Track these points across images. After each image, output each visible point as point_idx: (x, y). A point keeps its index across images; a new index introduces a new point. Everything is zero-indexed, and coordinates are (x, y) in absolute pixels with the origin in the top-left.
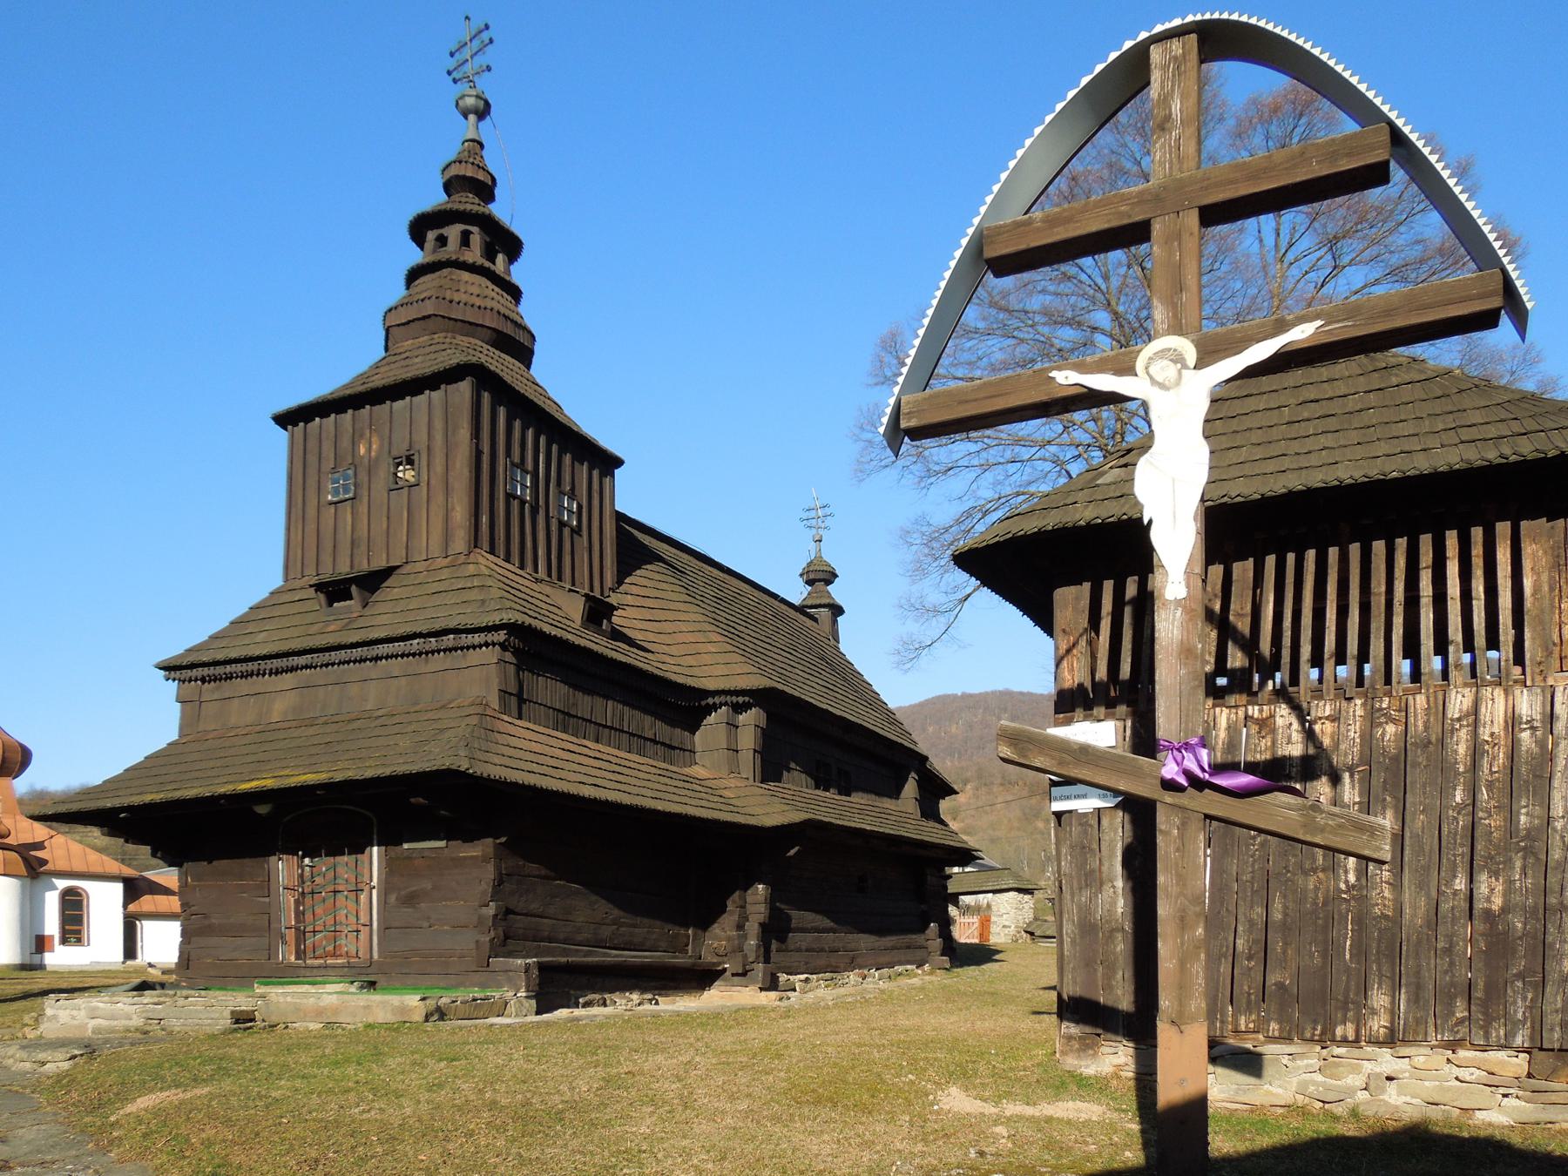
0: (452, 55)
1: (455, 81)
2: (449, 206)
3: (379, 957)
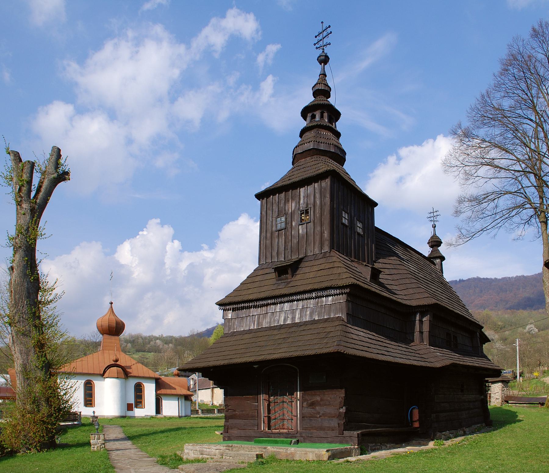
0: (316, 37)
1: (317, 48)
2: (316, 103)
3: (300, 430)
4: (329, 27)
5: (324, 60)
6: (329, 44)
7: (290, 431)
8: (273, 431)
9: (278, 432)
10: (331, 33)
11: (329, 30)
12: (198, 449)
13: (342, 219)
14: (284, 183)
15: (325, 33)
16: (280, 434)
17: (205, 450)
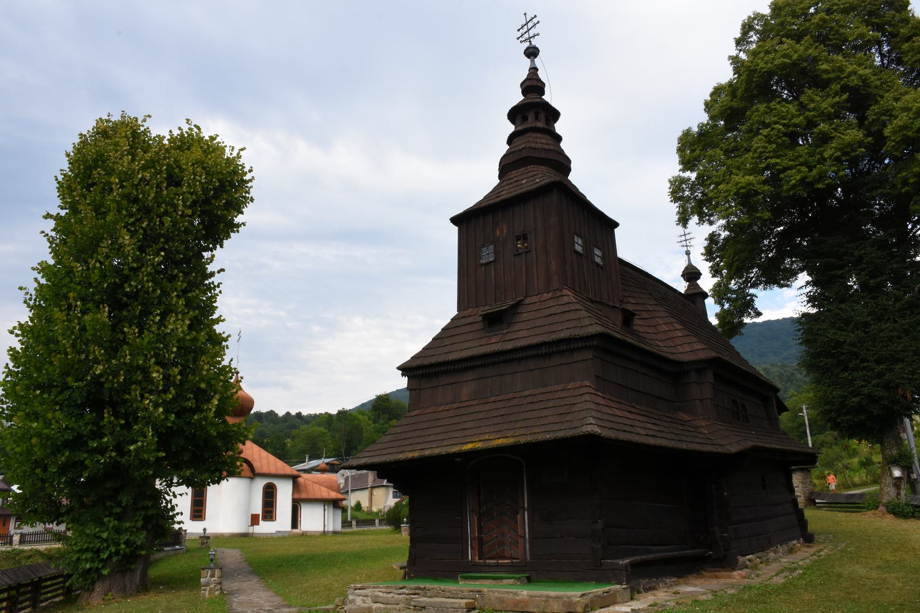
0: (519, 30)
1: (521, 42)
2: (527, 101)
3: (531, 558)
4: (535, 16)
5: (532, 53)
6: (538, 35)
7: (514, 561)
8: (487, 561)
9: (495, 563)
10: (538, 22)
11: (535, 20)
12: (370, 594)
13: (574, 245)
14: (491, 202)
15: (530, 25)
16: (498, 565)
17: (381, 594)
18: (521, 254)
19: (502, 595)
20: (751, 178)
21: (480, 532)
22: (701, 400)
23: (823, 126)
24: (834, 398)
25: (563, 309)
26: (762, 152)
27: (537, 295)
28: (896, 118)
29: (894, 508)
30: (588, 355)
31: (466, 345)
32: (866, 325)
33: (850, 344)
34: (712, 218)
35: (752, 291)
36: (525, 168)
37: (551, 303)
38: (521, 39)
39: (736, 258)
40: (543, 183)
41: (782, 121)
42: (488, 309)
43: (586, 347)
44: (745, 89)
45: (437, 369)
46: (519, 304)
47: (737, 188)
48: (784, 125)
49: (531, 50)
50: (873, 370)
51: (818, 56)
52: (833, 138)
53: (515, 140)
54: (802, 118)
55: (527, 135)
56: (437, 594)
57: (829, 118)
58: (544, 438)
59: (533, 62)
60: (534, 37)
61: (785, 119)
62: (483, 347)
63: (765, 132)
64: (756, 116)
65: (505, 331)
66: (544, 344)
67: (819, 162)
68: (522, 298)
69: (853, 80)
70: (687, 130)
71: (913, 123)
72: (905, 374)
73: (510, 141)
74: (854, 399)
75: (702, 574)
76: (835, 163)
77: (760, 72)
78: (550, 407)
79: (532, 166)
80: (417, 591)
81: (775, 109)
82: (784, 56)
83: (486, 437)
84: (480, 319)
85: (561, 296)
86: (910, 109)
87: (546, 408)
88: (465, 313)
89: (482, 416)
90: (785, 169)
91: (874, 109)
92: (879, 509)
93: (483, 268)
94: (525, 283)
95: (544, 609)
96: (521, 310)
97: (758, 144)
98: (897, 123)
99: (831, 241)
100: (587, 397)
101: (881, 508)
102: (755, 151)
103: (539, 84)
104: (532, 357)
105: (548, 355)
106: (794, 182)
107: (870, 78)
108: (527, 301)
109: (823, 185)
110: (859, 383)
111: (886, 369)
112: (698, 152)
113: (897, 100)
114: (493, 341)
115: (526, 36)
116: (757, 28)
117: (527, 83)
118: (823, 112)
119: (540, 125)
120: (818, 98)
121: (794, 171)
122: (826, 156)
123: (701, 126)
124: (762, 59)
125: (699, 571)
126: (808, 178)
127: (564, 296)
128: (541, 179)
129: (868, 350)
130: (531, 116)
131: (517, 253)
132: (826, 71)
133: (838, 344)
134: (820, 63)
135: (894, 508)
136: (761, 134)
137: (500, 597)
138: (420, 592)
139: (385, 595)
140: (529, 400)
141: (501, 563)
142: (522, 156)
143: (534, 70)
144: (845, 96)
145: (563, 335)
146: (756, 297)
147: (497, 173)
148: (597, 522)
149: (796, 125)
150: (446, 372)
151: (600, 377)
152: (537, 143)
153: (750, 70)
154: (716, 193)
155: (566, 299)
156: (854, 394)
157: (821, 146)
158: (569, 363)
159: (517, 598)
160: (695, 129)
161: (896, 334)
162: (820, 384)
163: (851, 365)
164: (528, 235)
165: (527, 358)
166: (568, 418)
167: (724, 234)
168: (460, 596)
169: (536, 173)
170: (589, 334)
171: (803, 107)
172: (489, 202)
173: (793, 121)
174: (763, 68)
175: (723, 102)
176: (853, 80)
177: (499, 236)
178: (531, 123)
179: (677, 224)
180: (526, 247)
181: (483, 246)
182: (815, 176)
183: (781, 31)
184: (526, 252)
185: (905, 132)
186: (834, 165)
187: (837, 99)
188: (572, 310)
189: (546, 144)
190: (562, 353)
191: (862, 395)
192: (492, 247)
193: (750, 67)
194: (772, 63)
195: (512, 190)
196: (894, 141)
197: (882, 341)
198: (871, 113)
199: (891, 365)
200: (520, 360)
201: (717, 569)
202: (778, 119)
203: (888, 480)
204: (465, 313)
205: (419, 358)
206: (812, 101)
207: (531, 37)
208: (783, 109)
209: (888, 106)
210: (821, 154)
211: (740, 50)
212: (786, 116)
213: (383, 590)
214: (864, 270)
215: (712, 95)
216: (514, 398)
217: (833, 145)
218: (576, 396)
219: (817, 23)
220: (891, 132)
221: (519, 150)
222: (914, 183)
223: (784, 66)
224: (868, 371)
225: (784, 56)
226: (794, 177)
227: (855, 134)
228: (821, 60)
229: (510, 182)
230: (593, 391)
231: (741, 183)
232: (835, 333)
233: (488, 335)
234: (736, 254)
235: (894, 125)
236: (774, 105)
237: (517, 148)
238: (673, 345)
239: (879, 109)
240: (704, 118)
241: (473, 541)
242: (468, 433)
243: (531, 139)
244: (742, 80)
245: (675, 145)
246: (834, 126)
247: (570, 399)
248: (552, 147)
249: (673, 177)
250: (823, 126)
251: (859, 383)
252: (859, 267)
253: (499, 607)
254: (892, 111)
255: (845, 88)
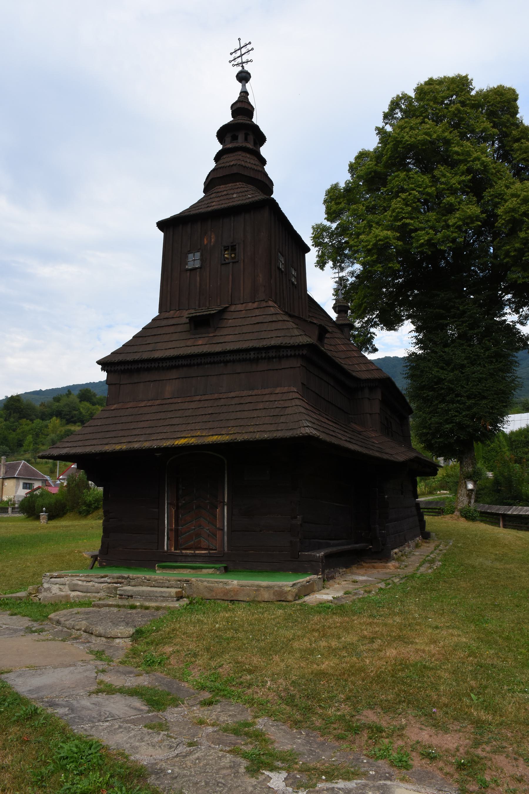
0: (231, 54)
1: (234, 65)
2: (236, 122)
3: (228, 550)
4: (250, 43)
6: (251, 61)
7: (211, 552)
8: (184, 551)
9: (192, 553)
10: (252, 49)
11: (249, 47)
12: (68, 582)
15: (244, 50)
16: (195, 556)
17: (80, 583)
18: (229, 263)
19: (212, 585)
20: (389, 233)
21: (177, 524)
22: (370, 414)
23: (452, 199)
24: (431, 423)
25: (270, 319)
26: (399, 212)
27: (242, 304)
28: (506, 201)
29: (467, 513)
30: (297, 363)
31: (170, 345)
32: (463, 366)
33: (450, 381)
34: (343, 265)
35: (372, 330)
36: (233, 184)
37: (257, 312)
38: (233, 62)
39: (365, 300)
40: (253, 199)
41: (418, 189)
42: (193, 312)
43: (295, 356)
44: (390, 157)
45: (140, 366)
46: (224, 311)
47: (376, 240)
48: (419, 192)
49: (244, 74)
50: (464, 403)
51: (451, 139)
52: (458, 210)
53: (224, 157)
54: (434, 188)
55: (236, 153)
56: (142, 583)
57: (453, 191)
58: (262, 437)
59: (244, 86)
60: (247, 62)
61: (420, 188)
62: (189, 348)
63: (403, 195)
64: (396, 181)
65: (212, 335)
66: (254, 349)
67: (443, 228)
68: (227, 305)
69: (477, 164)
70: (335, 184)
71: (519, 208)
72: (488, 408)
73: (218, 158)
74: (447, 426)
75: (362, 565)
76: (456, 230)
77: (405, 143)
78: (260, 409)
79: (240, 183)
80: (120, 580)
81: (413, 178)
82: (426, 134)
83: (198, 433)
84: (187, 321)
85: (267, 307)
86: (519, 196)
87: (257, 410)
88: (167, 315)
89: (188, 413)
90: (416, 230)
91: (490, 192)
92: (455, 513)
93: (188, 274)
94: (230, 291)
95: (254, 597)
96: (227, 316)
97: (396, 204)
98: (508, 205)
99: (443, 295)
100: (298, 402)
101: (457, 513)
102: (393, 211)
103: (250, 108)
104: (240, 361)
105: (256, 360)
106: (422, 241)
107: (490, 165)
108: (233, 308)
109: (445, 247)
110: (452, 412)
111: (474, 404)
112: (343, 205)
113: (507, 187)
114: (200, 342)
115: (239, 60)
116: (403, 107)
117: (239, 105)
118: (451, 187)
119: (250, 146)
120: (448, 174)
121: (423, 232)
122: (451, 224)
123: (347, 183)
124: (408, 133)
125: (359, 562)
126: (433, 240)
127: (270, 307)
128: (253, 195)
129: (463, 387)
130: (241, 137)
131: (224, 262)
132: (457, 153)
133: (440, 381)
134: (453, 145)
135: (467, 513)
136: (399, 197)
137: (209, 586)
138: (123, 581)
139: (85, 583)
140: (236, 401)
141: (198, 553)
142: (232, 172)
143: (244, 94)
144: (469, 177)
145: (273, 342)
146: (376, 335)
147: (202, 187)
148: (296, 518)
149: (428, 194)
150: (149, 370)
151: (304, 385)
152: (246, 162)
153: (396, 141)
154: (356, 242)
155: (272, 311)
156: (447, 422)
157: (446, 216)
158: (277, 370)
159: (227, 587)
160: (342, 185)
161: (484, 376)
162: (420, 411)
163: (448, 398)
164: (237, 246)
165: (234, 361)
166: (283, 419)
167: (351, 280)
168: (166, 585)
169: (246, 189)
170: (301, 344)
171: (435, 180)
172: (200, 211)
173: (426, 190)
174: (408, 141)
175: (369, 165)
176: (477, 164)
177: (207, 244)
178: (240, 142)
179: (316, 266)
180: (233, 258)
181: (190, 252)
182: (439, 239)
183: (424, 113)
184: (233, 263)
185: (513, 214)
186: (456, 232)
187: (463, 178)
188: (279, 321)
189: (255, 164)
190: (270, 359)
191: (454, 423)
192: (198, 255)
193: (397, 138)
194: (416, 139)
195: (223, 202)
196: (504, 219)
197: (474, 381)
198: (487, 194)
199: (478, 400)
200: (226, 363)
201: (374, 561)
202: (415, 186)
203: (463, 492)
204: (167, 315)
205: (121, 353)
206: (444, 176)
207: (244, 63)
208: (419, 178)
209: (501, 191)
210: (445, 221)
211: (386, 124)
212: (421, 185)
213: (83, 578)
214: (463, 322)
215: (357, 158)
216: (220, 399)
217: (457, 215)
218: (286, 400)
219: (454, 112)
220: (503, 212)
221: (229, 166)
222: (514, 256)
223: (424, 143)
224: (461, 404)
225: (426, 134)
226: (423, 237)
227: (474, 210)
228: (453, 143)
229: (220, 194)
230: (301, 397)
231: (379, 235)
232: (438, 371)
233: (193, 337)
234: (365, 296)
235: (505, 207)
236: (412, 175)
237: (228, 164)
238: (351, 364)
239: (493, 192)
240: (348, 177)
241: (169, 532)
242: (177, 428)
243: (240, 157)
244: (388, 149)
245: (322, 196)
246: (458, 200)
247: (280, 402)
248: (260, 169)
249: (316, 225)
250: (452, 199)
251: (452, 412)
252: (462, 319)
253: (208, 596)
254: (504, 195)
255: (469, 171)
